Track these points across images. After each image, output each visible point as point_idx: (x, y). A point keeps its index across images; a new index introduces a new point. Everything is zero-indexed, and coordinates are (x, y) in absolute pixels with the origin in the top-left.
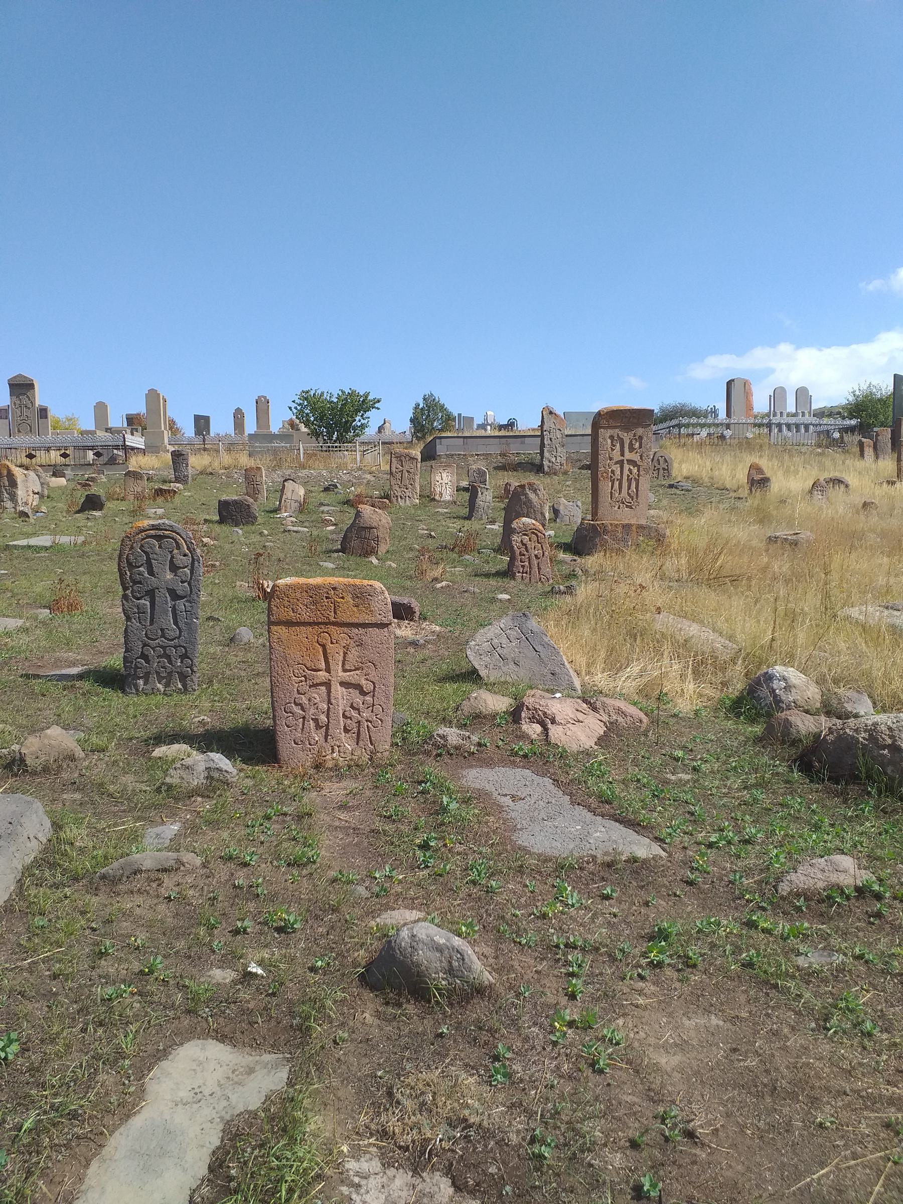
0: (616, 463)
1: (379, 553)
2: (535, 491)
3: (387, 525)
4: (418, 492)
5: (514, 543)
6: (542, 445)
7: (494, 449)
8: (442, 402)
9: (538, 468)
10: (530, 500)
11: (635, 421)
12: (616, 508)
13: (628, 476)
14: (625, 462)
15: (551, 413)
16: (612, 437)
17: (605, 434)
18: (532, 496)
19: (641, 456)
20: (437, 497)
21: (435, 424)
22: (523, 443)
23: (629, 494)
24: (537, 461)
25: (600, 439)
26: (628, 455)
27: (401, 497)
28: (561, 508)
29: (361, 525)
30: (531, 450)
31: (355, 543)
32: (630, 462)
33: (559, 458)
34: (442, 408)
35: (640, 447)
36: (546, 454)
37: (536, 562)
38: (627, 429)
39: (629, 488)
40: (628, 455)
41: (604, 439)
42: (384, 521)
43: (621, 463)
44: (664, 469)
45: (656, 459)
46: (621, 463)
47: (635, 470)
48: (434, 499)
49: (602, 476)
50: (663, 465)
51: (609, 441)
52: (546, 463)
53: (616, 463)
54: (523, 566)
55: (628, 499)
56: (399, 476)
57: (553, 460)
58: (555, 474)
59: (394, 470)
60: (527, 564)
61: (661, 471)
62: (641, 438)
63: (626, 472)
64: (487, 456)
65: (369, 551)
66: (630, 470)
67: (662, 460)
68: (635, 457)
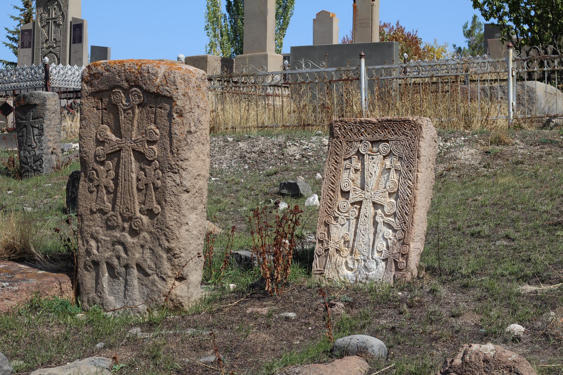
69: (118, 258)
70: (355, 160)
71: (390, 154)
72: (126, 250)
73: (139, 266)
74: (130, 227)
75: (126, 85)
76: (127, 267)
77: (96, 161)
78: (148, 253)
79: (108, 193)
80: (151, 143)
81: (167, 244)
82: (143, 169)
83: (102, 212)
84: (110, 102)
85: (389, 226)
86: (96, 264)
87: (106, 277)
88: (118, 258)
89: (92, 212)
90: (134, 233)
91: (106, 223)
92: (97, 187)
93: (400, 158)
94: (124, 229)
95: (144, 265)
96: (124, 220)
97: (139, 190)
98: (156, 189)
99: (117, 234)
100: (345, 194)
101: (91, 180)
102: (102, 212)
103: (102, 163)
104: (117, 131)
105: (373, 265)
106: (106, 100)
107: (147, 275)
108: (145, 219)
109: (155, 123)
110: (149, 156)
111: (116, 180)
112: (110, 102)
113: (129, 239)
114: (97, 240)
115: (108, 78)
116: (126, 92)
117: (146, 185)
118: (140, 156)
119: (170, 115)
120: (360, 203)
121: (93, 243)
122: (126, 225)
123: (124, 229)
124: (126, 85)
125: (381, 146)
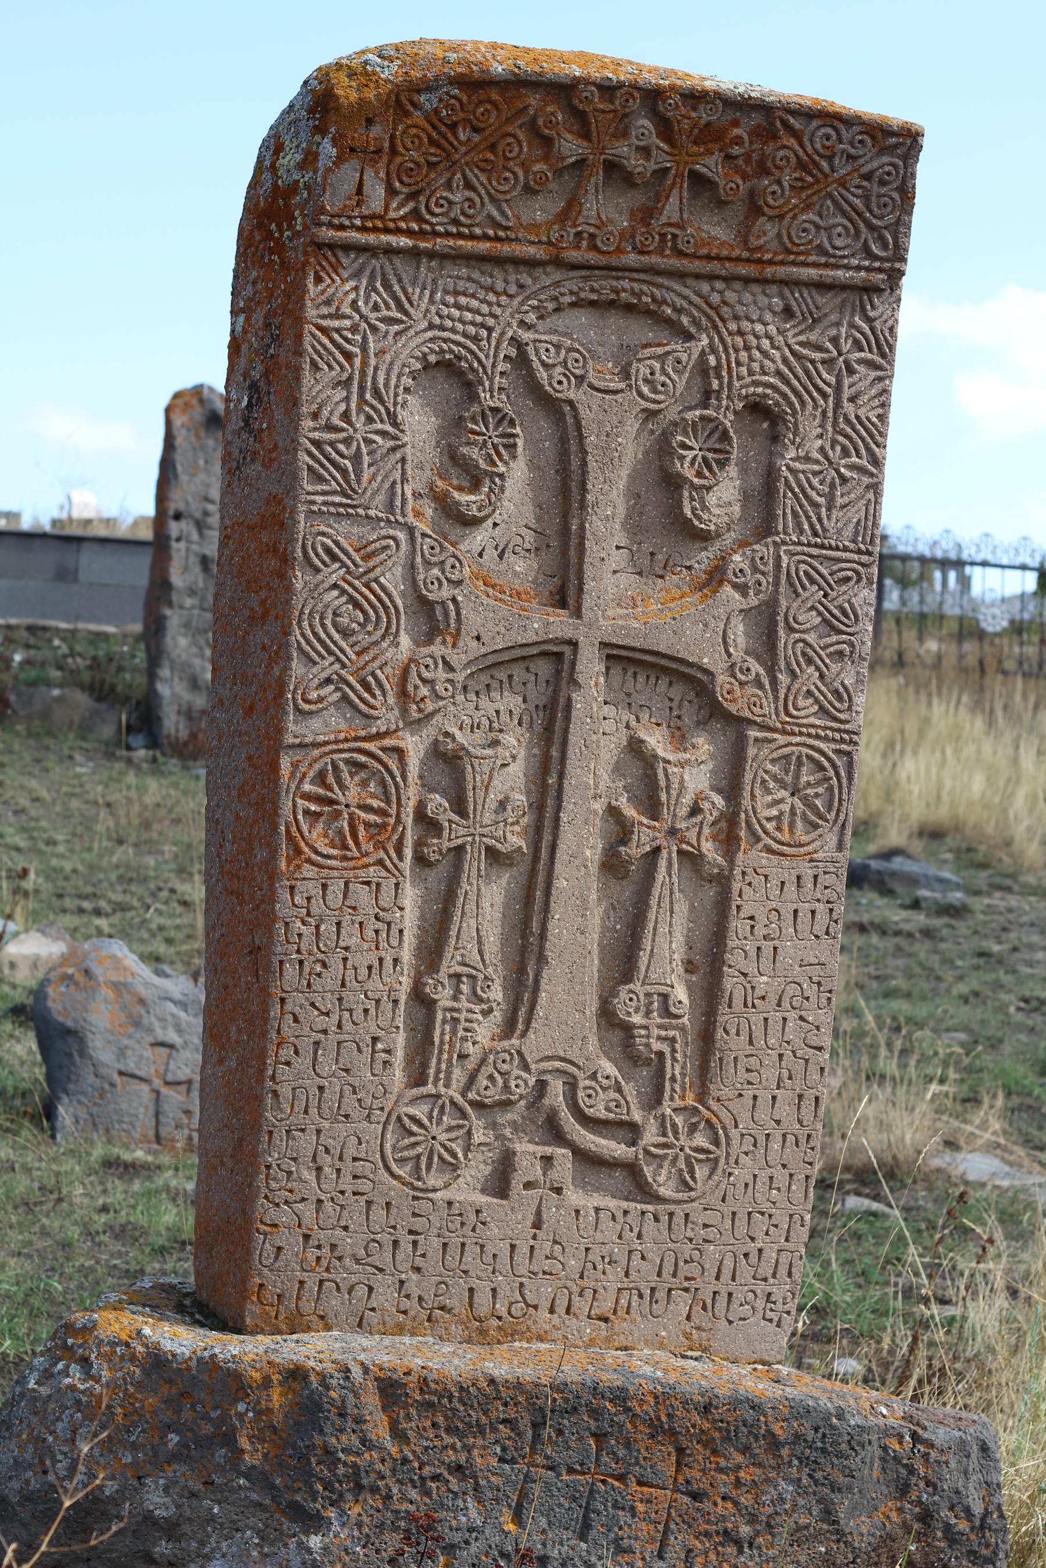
11: (716, 230)
12: (467, 1189)
19: (767, 624)
22: (65, 575)
24: (132, 679)
26: (619, 599)
28: (100, 1019)
35: (763, 522)
38: (619, 289)
39: (624, 959)
47: (693, 773)
51: (419, 422)
63: (594, 778)
68: (710, 633)
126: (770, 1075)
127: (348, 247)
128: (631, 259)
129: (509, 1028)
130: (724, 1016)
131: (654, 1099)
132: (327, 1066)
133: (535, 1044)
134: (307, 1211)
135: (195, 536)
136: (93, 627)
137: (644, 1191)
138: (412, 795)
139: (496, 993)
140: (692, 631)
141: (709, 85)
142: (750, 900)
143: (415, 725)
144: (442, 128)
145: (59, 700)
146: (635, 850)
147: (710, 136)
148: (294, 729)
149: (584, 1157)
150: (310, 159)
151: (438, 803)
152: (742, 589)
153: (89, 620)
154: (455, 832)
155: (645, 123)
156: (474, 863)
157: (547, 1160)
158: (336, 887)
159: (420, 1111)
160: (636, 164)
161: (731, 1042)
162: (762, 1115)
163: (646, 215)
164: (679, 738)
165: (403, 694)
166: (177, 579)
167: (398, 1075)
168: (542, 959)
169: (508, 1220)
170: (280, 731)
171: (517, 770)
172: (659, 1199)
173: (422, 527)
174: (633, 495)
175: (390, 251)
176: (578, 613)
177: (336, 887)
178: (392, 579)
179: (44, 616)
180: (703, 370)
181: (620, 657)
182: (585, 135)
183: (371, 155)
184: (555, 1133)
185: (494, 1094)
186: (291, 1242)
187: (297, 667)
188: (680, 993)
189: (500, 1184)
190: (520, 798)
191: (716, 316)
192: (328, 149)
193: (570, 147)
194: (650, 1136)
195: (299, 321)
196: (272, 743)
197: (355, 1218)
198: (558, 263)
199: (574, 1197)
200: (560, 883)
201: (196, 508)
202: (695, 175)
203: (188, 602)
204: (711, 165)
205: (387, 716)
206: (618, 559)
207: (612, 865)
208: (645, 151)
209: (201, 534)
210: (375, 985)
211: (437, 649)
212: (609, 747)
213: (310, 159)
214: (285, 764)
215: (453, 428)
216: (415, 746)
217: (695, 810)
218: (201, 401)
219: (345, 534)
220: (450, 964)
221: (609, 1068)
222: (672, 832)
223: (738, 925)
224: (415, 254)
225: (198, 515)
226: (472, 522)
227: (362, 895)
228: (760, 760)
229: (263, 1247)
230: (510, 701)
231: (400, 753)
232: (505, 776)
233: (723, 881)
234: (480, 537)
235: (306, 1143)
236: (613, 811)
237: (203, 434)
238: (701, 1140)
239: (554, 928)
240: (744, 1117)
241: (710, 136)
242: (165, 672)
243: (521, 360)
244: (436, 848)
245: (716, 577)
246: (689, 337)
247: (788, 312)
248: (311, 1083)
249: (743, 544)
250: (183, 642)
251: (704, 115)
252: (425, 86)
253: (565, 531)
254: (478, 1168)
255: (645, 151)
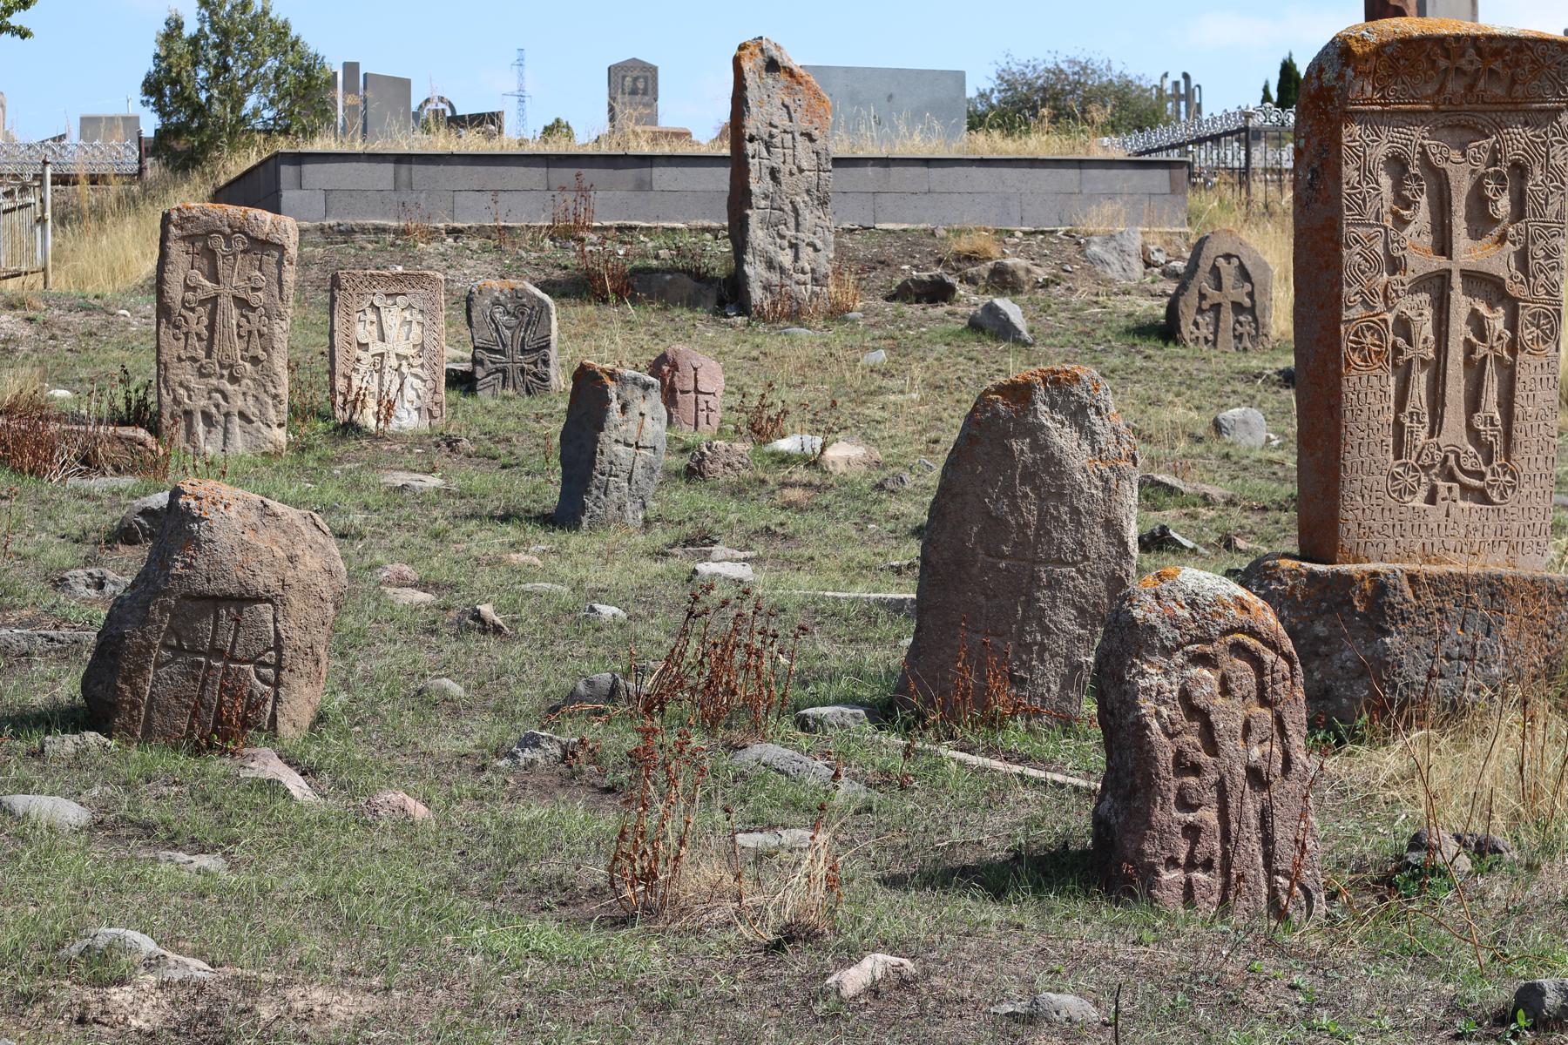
0: (1419, 285)
1: (285, 728)
2: (1078, 415)
3: (323, 583)
4: (283, 391)
5: (1147, 706)
6: (739, 198)
7: (528, 206)
8: (278, 13)
9: (728, 295)
10: (1051, 462)
11: (1498, 91)
12: (1418, 502)
13: (1470, 348)
14: (1457, 281)
15: (772, 66)
16: (1397, 164)
17: (1368, 148)
18: (1064, 438)
19: (1523, 259)
20: (368, 419)
21: (251, 101)
22: (643, 186)
23: (1474, 435)
25: (1350, 172)
26: (1469, 252)
27: (208, 418)
29: (200, 585)
30: (685, 217)
31: (158, 679)
32: (1478, 281)
33: (806, 253)
34: (281, 37)
35: (1519, 212)
36: (758, 235)
37: (1252, 808)
38: (1462, 123)
40: (1469, 252)
41: (1367, 173)
42: (311, 562)
43: (1438, 286)
44: (1238, 307)
45: (1205, 265)
46: (1438, 286)
47: (1497, 321)
48: (350, 429)
49: (1359, 347)
50: (1234, 291)
51: (1386, 182)
52: (754, 270)
53: (1419, 285)
54: (1192, 832)
55: (1471, 458)
56: (197, 322)
57: (786, 258)
58: (795, 315)
59: (175, 292)
60: (1209, 816)
61: (1228, 317)
62: (1520, 170)
63: (1460, 330)
64: (499, 237)
65: (227, 723)
66: (1477, 323)
67: (1228, 271)
68: (1495, 259)
69: (217, 406)
70: (369, 311)
71: (410, 306)
72: (225, 398)
73: (242, 415)
74: (231, 374)
75: (228, 231)
76: (227, 415)
77: (184, 306)
78: (250, 400)
79: (200, 339)
80: (254, 289)
81: (274, 391)
82: (246, 317)
83: (194, 359)
84: (206, 247)
85: (416, 376)
86: (188, 414)
87: (200, 428)
88: (217, 406)
89: (180, 359)
90: (234, 380)
91: (199, 370)
92: (186, 334)
93: (421, 311)
94: (222, 376)
95: (248, 413)
96: (222, 366)
97: (240, 337)
98: (261, 335)
99: (214, 381)
100: (364, 346)
101: (179, 328)
102: (194, 359)
103: (193, 310)
104: (214, 277)
105: (405, 415)
106: (199, 245)
107: (250, 422)
108: (248, 366)
109: (260, 270)
110: (254, 302)
111: (211, 327)
112: (206, 247)
113: (229, 387)
114: (187, 389)
115: (206, 222)
116: (228, 238)
117: (250, 332)
118: (242, 303)
119: (280, 264)
120: (382, 355)
121: (181, 391)
122: (225, 372)
123: (222, 376)
124: (228, 231)
125: (399, 299)
126: (1534, 449)
127: (1357, 112)
128: (1466, 107)
129: (1431, 434)
130: (1515, 424)
131: (1488, 462)
132: (1364, 453)
133: (1444, 439)
134: (1359, 513)
135: (765, 154)
136: (666, 224)
137: (1486, 500)
138: (1391, 337)
139: (1427, 419)
140: (1495, 262)
141: (1496, 32)
142: (1523, 375)
143: (1390, 310)
144: (1393, 60)
145: (670, 283)
146: (1477, 356)
147: (1498, 53)
148: (1346, 315)
149: (1465, 488)
150: (1341, 77)
151: (1401, 341)
152: (1513, 243)
153: (664, 220)
154: (1409, 353)
155: (1472, 51)
156: (1416, 366)
157: (1450, 489)
158: (1364, 379)
159: (1400, 470)
160: (1467, 68)
161: (1519, 436)
162: (1532, 466)
163: (1471, 87)
164: (1491, 307)
165: (1386, 297)
166: (754, 187)
167: (1392, 456)
168: (1444, 405)
169: (1436, 513)
170: (1340, 315)
171: (1429, 325)
172: (1493, 503)
173: (1390, 226)
174: (1467, 205)
175: (1373, 112)
176: (1450, 258)
177: (1364, 379)
178: (1379, 249)
179: (629, 218)
180: (1494, 151)
181: (1469, 276)
182: (1448, 57)
183: (1367, 75)
184: (1451, 477)
185: (1428, 462)
186: (1353, 526)
187: (1345, 289)
188: (1497, 416)
189: (1431, 498)
190: (1432, 337)
191: (1499, 126)
192: (1350, 72)
193: (1443, 63)
194: (1489, 477)
195: (1340, 144)
196: (1337, 320)
197: (1377, 515)
198: (1436, 110)
199: (1461, 504)
200: (1449, 372)
201: (764, 132)
202: (1491, 70)
203: (763, 203)
204: (1497, 65)
205: (1380, 306)
206: (1464, 232)
207: (1468, 362)
208: (1471, 62)
209: (769, 152)
210: (1381, 418)
211: (1398, 276)
212: (1464, 313)
213: (1341, 77)
214: (1342, 328)
215: (1398, 186)
216: (1390, 317)
217: (1500, 338)
218: (762, 50)
219: (1361, 232)
220: (1409, 409)
221: (1471, 449)
222: (1491, 347)
223: (1519, 386)
224: (1382, 112)
225: (766, 137)
226: (1407, 223)
227: (1374, 381)
228: (1524, 316)
229: (1343, 530)
230: (1425, 297)
231: (1385, 321)
232: (1425, 328)
233: (1512, 367)
234: (1411, 228)
235: (1357, 485)
236: (1467, 341)
237: (764, 74)
238: (1508, 478)
239: (1448, 390)
240: (1525, 467)
241: (1498, 53)
242: (749, 258)
243: (1424, 153)
244: (1401, 359)
245: (1502, 239)
246: (1487, 137)
247: (1526, 124)
248: (1358, 460)
249: (1512, 223)
250: (760, 233)
251: (1495, 45)
252: (1388, 44)
253: (1443, 222)
254: (1423, 493)
255: (1471, 62)
